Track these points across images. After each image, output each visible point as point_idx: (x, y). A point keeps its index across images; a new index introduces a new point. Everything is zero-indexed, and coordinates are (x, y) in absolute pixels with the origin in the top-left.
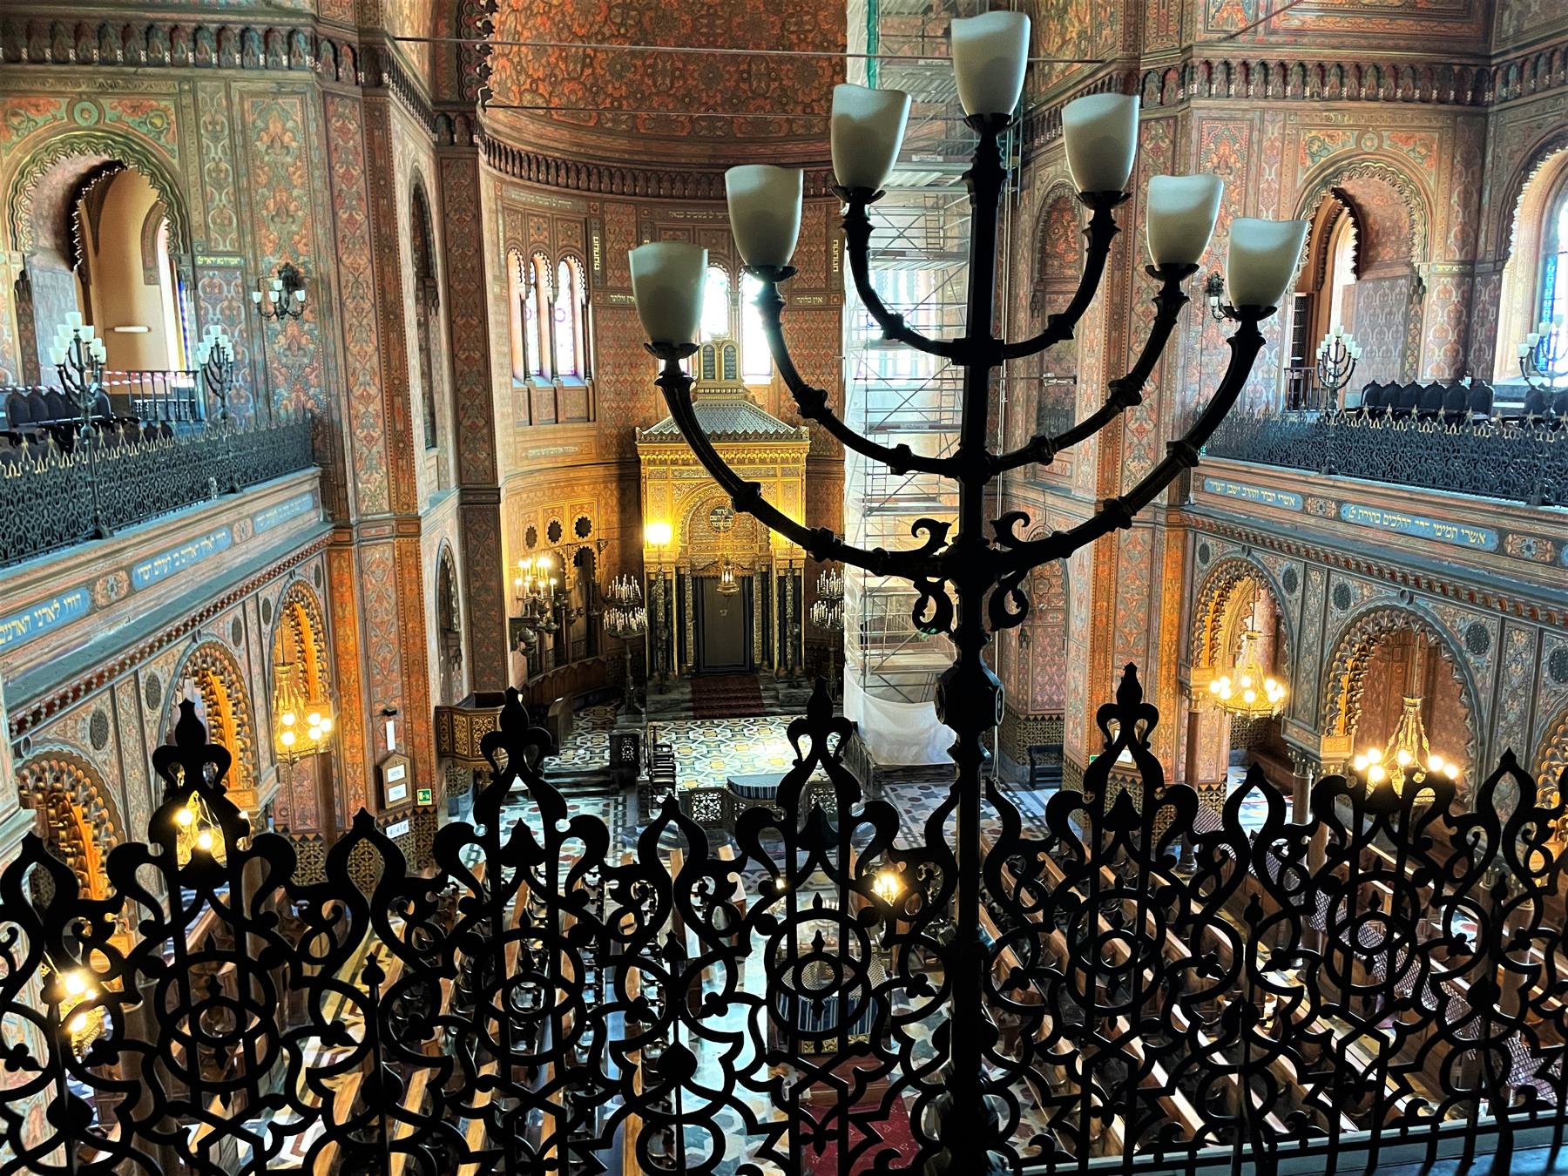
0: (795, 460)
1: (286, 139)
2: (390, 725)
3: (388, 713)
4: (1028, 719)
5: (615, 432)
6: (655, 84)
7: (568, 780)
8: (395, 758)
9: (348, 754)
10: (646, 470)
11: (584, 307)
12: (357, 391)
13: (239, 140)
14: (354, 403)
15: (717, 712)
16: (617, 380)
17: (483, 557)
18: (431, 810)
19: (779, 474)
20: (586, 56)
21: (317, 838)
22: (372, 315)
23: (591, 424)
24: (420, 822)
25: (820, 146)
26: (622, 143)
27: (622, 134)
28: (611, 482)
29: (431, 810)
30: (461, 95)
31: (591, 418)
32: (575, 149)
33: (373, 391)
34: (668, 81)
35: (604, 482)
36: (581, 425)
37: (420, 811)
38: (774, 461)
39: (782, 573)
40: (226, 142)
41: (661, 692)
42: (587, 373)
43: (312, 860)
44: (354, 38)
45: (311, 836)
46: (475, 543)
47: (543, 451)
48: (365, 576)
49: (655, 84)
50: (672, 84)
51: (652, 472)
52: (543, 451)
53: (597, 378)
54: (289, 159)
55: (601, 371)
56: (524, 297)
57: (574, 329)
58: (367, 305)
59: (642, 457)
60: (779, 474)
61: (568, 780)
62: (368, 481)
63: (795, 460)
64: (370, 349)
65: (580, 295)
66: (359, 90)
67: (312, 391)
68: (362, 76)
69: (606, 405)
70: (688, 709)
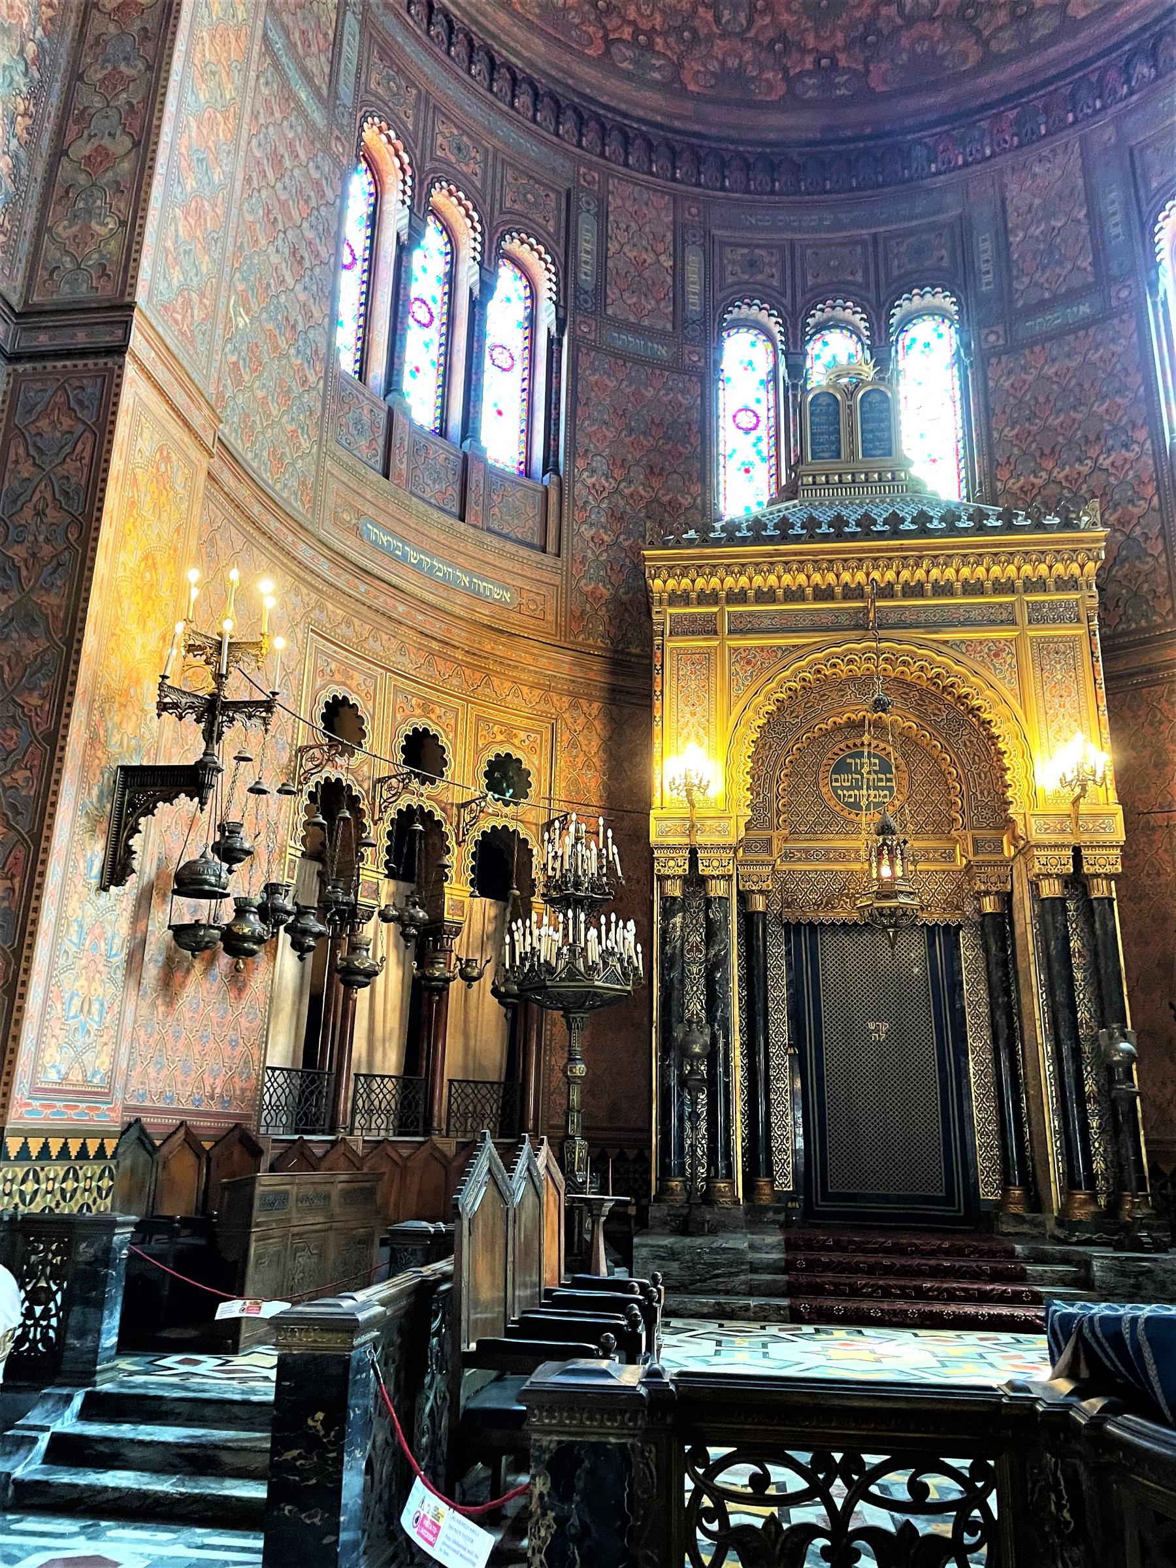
0: (1070, 584)
5: (605, 591)
6: (718, 20)
7: (169, 1434)
10: (664, 615)
11: (554, 344)
15: (873, 1307)
16: (616, 491)
17: (40, 514)
19: (1022, 616)
23: (548, 560)
26: (655, 99)
27: (654, 85)
28: (590, 699)
31: (551, 547)
34: (742, 17)
35: (570, 693)
36: (524, 552)
38: (1007, 587)
39: (1050, 889)
41: (684, 1228)
42: (550, 464)
46: (26, 470)
49: (718, 20)
50: (751, 21)
53: (571, 473)
55: (580, 463)
56: (404, 238)
57: (530, 392)
59: (657, 584)
60: (1022, 616)
61: (169, 1434)
69: (588, 533)
70: (769, 1291)
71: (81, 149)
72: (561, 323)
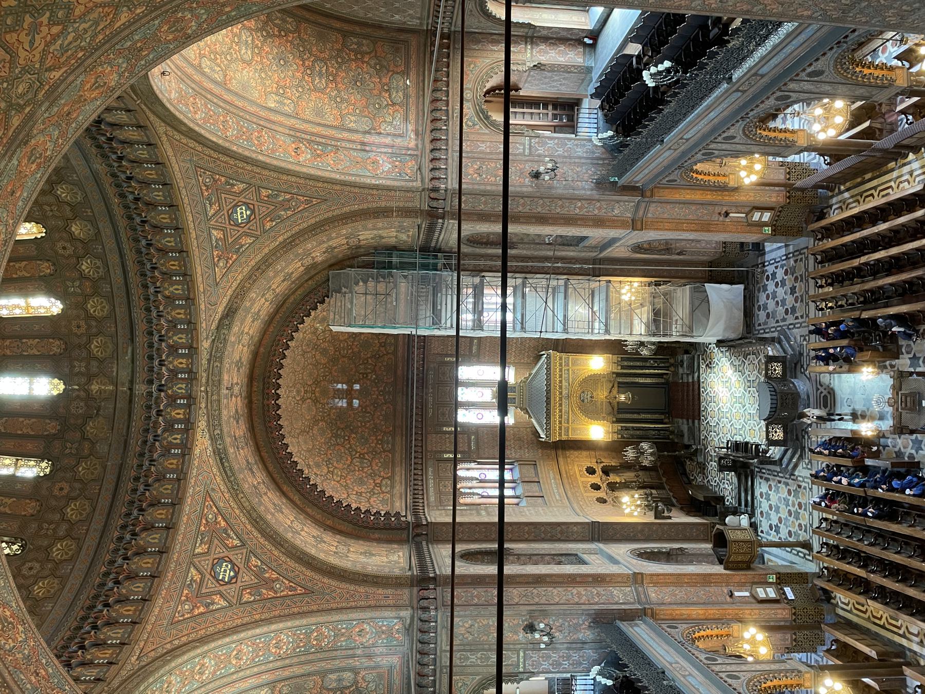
0: (561, 359)
1: (467, 626)
2: (737, 594)
3: (731, 595)
4: (725, 252)
5: (540, 451)
6: (369, 422)
7: (743, 495)
8: (753, 592)
9: (754, 617)
10: (564, 438)
11: (479, 463)
12: (576, 600)
13: (467, 648)
14: (582, 602)
15: (696, 407)
18: (778, 576)
20: (359, 457)
21: (795, 634)
22: (540, 589)
23: (538, 464)
24: (784, 581)
25: (400, 339)
26: (398, 439)
27: (393, 438)
28: (566, 454)
29: (778, 576)
30: (404, 529)
32: (404, 465)
33: (575, 591)
34: (368, 415)
35: (566, 457)
37: (778, 581)
38: (561, 370)
39: (619, 368)
40: (469, 654)
41: (682, 436)
43: (806, 637)
44: (415, 590)
45: (794, 637)
46: (618, 535)
47: (556, 491)
48: (665, 602)
49: (369, 422)
50: (368, 413)
51: (565, 435)
52: (556, 491)
53: (514, 459)
54: (476, 625)
57: (488, 469)
58: (535, 591)
61: (743, 495)
62: (618, 597)
63: (561, 359)
64: (555, 591)
65: (473, 465)
66: (438, 588)
67: (581, 622)
68: (431, 586)
69: (527, 455)
70: (693, 422)
71: (559, 536)
72: (475, 462)
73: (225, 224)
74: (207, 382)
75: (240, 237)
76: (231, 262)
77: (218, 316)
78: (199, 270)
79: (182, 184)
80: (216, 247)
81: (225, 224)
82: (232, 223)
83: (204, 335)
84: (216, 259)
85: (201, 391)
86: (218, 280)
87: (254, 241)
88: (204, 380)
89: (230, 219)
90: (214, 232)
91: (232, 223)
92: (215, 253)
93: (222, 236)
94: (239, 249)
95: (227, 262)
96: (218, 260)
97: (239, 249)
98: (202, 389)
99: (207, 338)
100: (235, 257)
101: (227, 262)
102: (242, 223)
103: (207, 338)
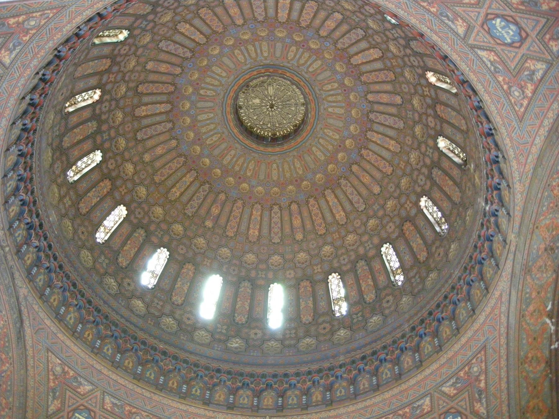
73: (87, 402)
74: (6, 257)
75: (63, 403)
76: (51, 377)
77: (26, 323)
78: (75, 349)
79: (156, 397)
80: (76, 378)
81: (87, 402)
82: (82, 407)
83: (30, 299)
84: (66, 369)
85: (8, 246)
86: (50, 354)
87: (47, 411)
88: (9, 257)
89: (87, 408)
90: (88, 388)
91: (82, 407)
92: (72, 373)
93: (79, 390)
94: (54, 393)
95: (54, 374)
96: (64, 369)
97: (54, 393)
98: (7, 249)
99: (25, 298)
100: (52, 384)
101: (54, 374)
102: (73, 415)
103: (25, 298)
